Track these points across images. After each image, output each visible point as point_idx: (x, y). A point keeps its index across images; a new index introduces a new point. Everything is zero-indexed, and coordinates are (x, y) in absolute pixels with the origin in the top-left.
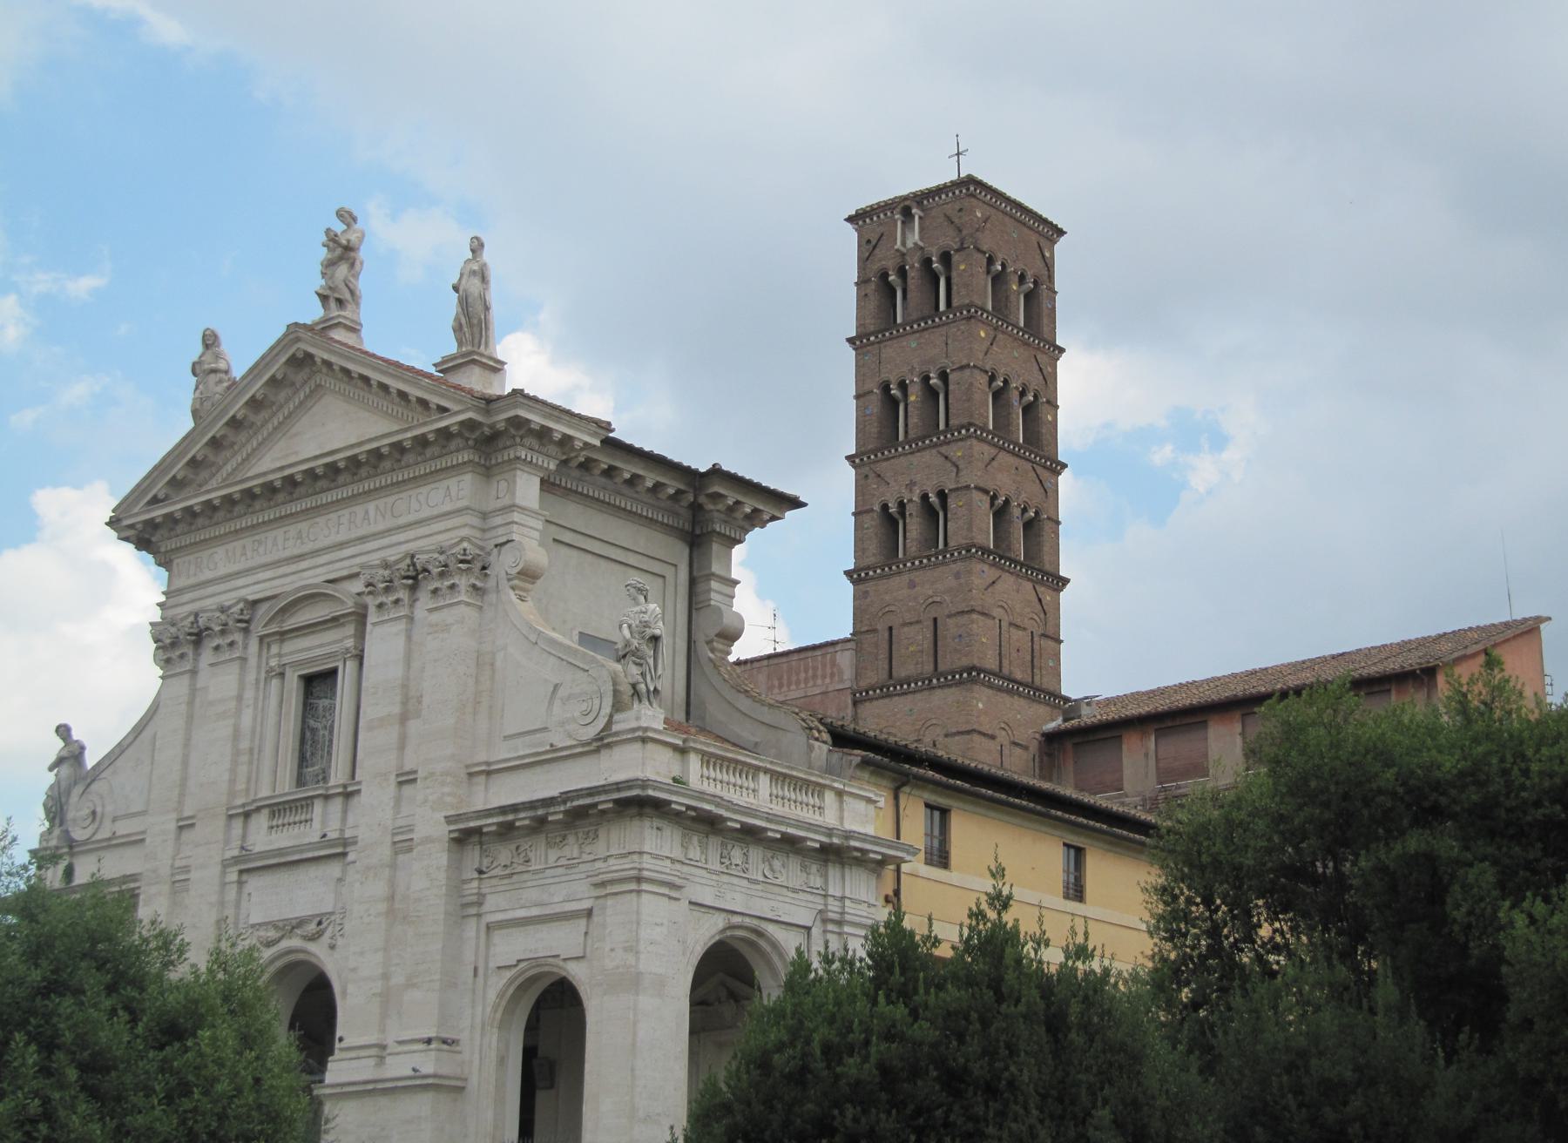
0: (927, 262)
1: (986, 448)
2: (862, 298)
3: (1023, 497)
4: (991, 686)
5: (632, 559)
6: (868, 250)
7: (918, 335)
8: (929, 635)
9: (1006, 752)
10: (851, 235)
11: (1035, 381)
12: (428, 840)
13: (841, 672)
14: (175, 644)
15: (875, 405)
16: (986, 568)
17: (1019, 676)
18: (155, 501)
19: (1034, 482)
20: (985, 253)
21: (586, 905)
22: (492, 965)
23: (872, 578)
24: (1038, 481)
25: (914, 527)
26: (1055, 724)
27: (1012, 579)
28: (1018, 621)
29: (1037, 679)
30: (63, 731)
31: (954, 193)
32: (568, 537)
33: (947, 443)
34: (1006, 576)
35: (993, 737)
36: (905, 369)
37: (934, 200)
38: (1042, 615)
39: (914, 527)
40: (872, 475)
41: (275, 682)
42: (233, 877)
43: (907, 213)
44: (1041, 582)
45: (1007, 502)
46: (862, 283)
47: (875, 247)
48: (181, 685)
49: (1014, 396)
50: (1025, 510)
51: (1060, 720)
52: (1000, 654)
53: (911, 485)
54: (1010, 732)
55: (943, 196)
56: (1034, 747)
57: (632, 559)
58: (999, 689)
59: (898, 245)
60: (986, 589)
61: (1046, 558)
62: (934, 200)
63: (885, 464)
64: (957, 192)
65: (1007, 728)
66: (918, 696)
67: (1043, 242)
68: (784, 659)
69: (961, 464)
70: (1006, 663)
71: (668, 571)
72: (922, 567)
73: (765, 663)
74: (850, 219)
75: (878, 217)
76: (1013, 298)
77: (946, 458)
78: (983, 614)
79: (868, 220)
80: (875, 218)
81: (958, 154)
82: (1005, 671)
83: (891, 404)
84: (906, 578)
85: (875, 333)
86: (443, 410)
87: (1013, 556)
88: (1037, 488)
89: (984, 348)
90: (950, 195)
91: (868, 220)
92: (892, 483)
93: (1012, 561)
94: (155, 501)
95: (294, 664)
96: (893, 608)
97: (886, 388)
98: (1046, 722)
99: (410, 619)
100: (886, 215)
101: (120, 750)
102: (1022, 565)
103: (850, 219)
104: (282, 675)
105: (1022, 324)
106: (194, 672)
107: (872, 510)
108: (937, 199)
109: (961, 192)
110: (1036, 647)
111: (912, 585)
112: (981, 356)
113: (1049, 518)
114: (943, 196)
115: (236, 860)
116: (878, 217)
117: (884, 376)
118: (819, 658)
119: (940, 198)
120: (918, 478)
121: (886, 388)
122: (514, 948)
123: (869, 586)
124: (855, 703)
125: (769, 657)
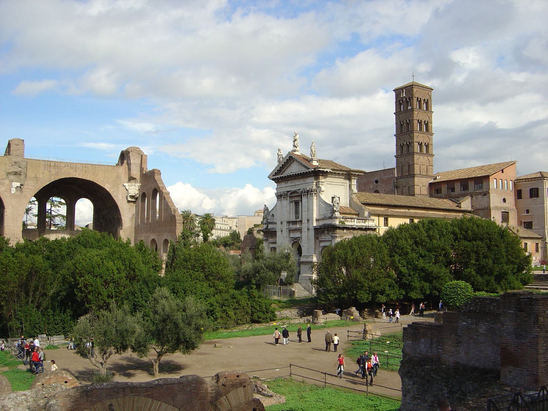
0: (406, 99)
1: (418, 134)
2: (396, 105)
3: (425, 141)
4: (418, 177)
5: (339, 184)
6: (397, 96)
9: (421, 188)
10: (394, 93)
11: (427, 119)
12: (311, 229)
14: (278, 196)
15: (399, 125)
16: (417, 156)
18: (273, 175)
21: (331, 239)
22: (320, 246)
25: (405, 148)
26: (432, 181)
27: (423, 157)
28: (424, 164)
29: (428, 174)
30: (265, 205)
32: (329, 183)
34: (421, 157)
36: (403, 119)
39: (405, 148)
41: (291, 203)
42: (288, 230)
43: (403, 90)
44: (429, 156)
45: (421, 143)
46: (396, 102)
48: (280, 202)
49: (423, 123)
50: (425, 144)
51: (433, 180)
56: (427, 186)
57: (339, 184)
58: (420, 177)
59: (402, 96)
61: (430, 151)
67: (429, 92)
71: (346, 184)
72: (406, 156)
74: (393, 90)
76: (422, 104)
77: (410, 136)
81: (413, 76)
82: (421, 173)
83: (402, 125)
84: (404, 157)
85: (398, 112)
86: (309, 168)
87: (423, 153)
93: (423, 154)
94: (273, 175)
95: (294, 201)
97: (400, 122)
98: (430, 181)
99: (308, 197)
101: (273, 209)
102: (426, 154)
103: (393, 90)
104: (292, 202)
105: (425, 109)
106: (281, 200)
111: (405, 159)
112: (416, 117)
115: (288, 228)
117: (400, 120)
120: (405, 139)
121: (400, 122)
122: (322, 244)
123: (398, 159)
124: (396, 179)
125: (383, 170)
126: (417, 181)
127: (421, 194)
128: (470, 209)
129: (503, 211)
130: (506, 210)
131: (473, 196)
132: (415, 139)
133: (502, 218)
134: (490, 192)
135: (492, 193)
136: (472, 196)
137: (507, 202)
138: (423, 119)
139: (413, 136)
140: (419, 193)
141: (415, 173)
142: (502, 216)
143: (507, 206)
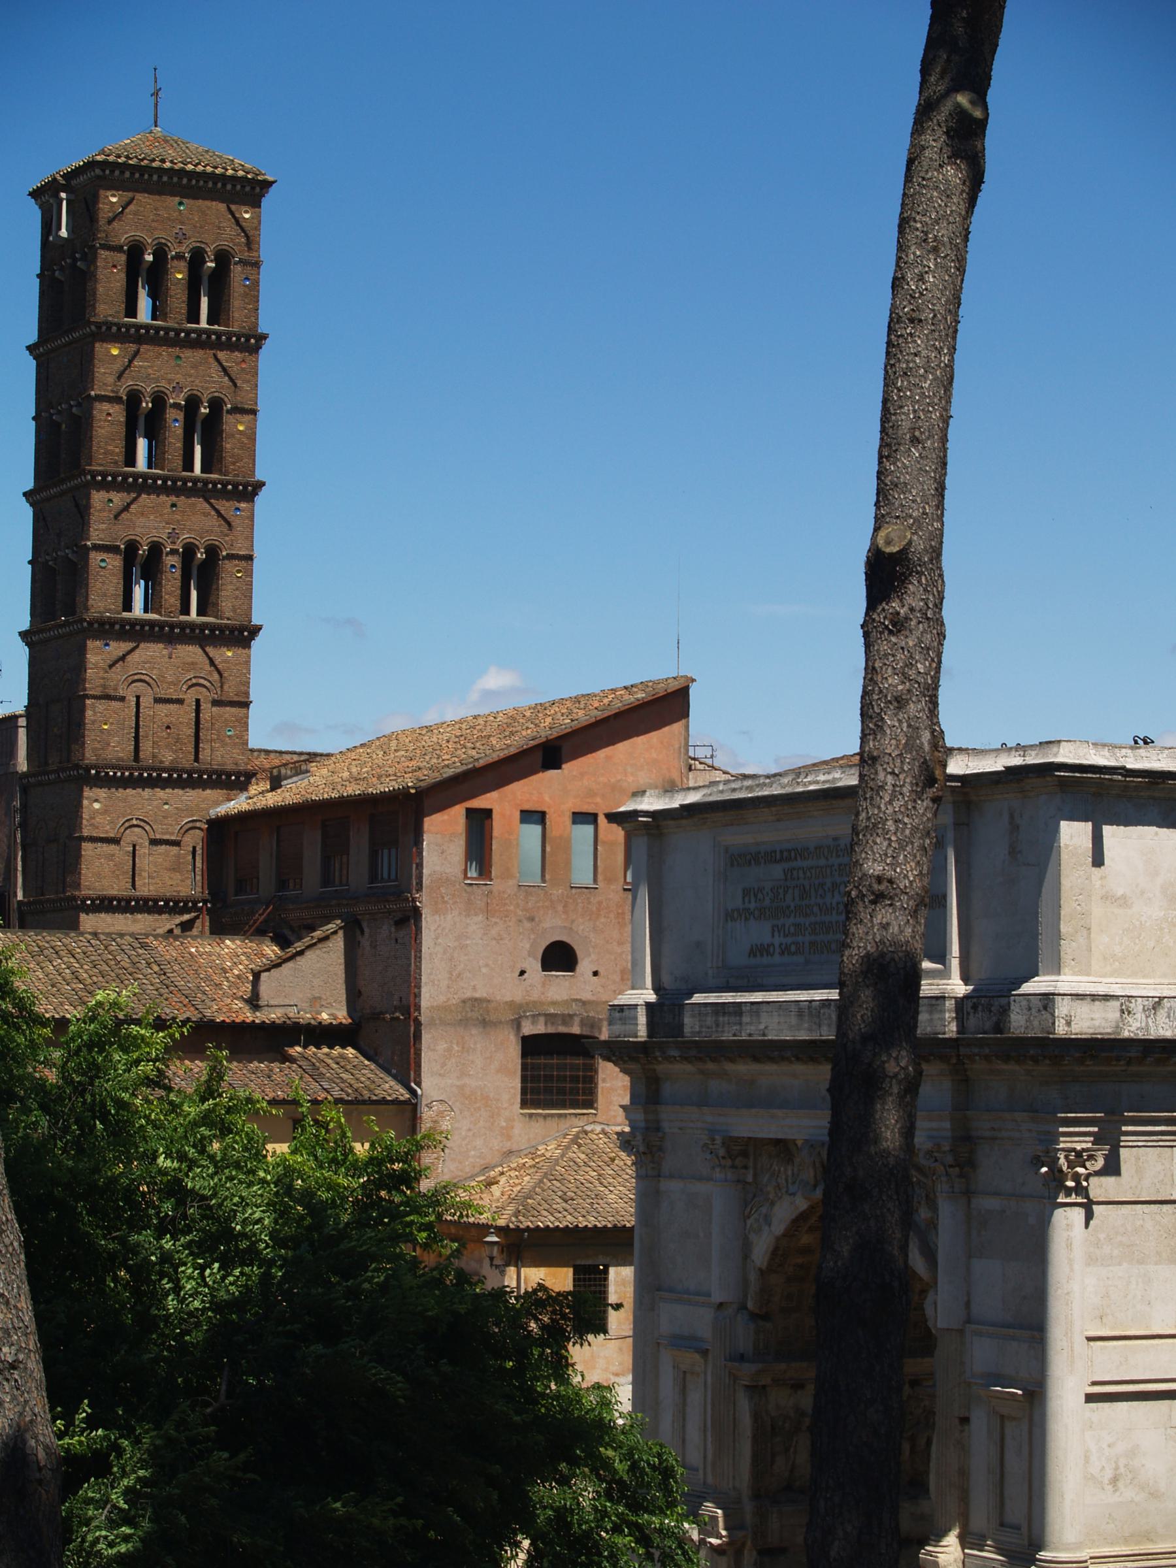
17: (168, 757)
19: (207, 515)
20: (119, 249)
24: (213, 513)
35: (115, 841)
38: (216, 676)
52: (137, 738)
54: (148, 828)
56: (195, 838)
60: (111, 666)
65: (142, 824)
70: (146, 748)
78: (108, 697)
88: (213, 521)
89: (118, 366)
110: (205, 716)
112: (111, 380)
113: (231, 557)
126: (105, 811)
127: (145, 888)
128: (334, 1012)
129: (540, 1028)
130: (567, 1019)
131: (365, 925)
132: (98, 532)
133: (524, 1079)
134: (425, 901)
135: (436, 912)
136: (353, 931)
137: (585, 966)
138: (178, 388)
139: (88, 506)
140: (117, 887)
141: (90, 757)
142: (524, 1067)
143: (586, 996)
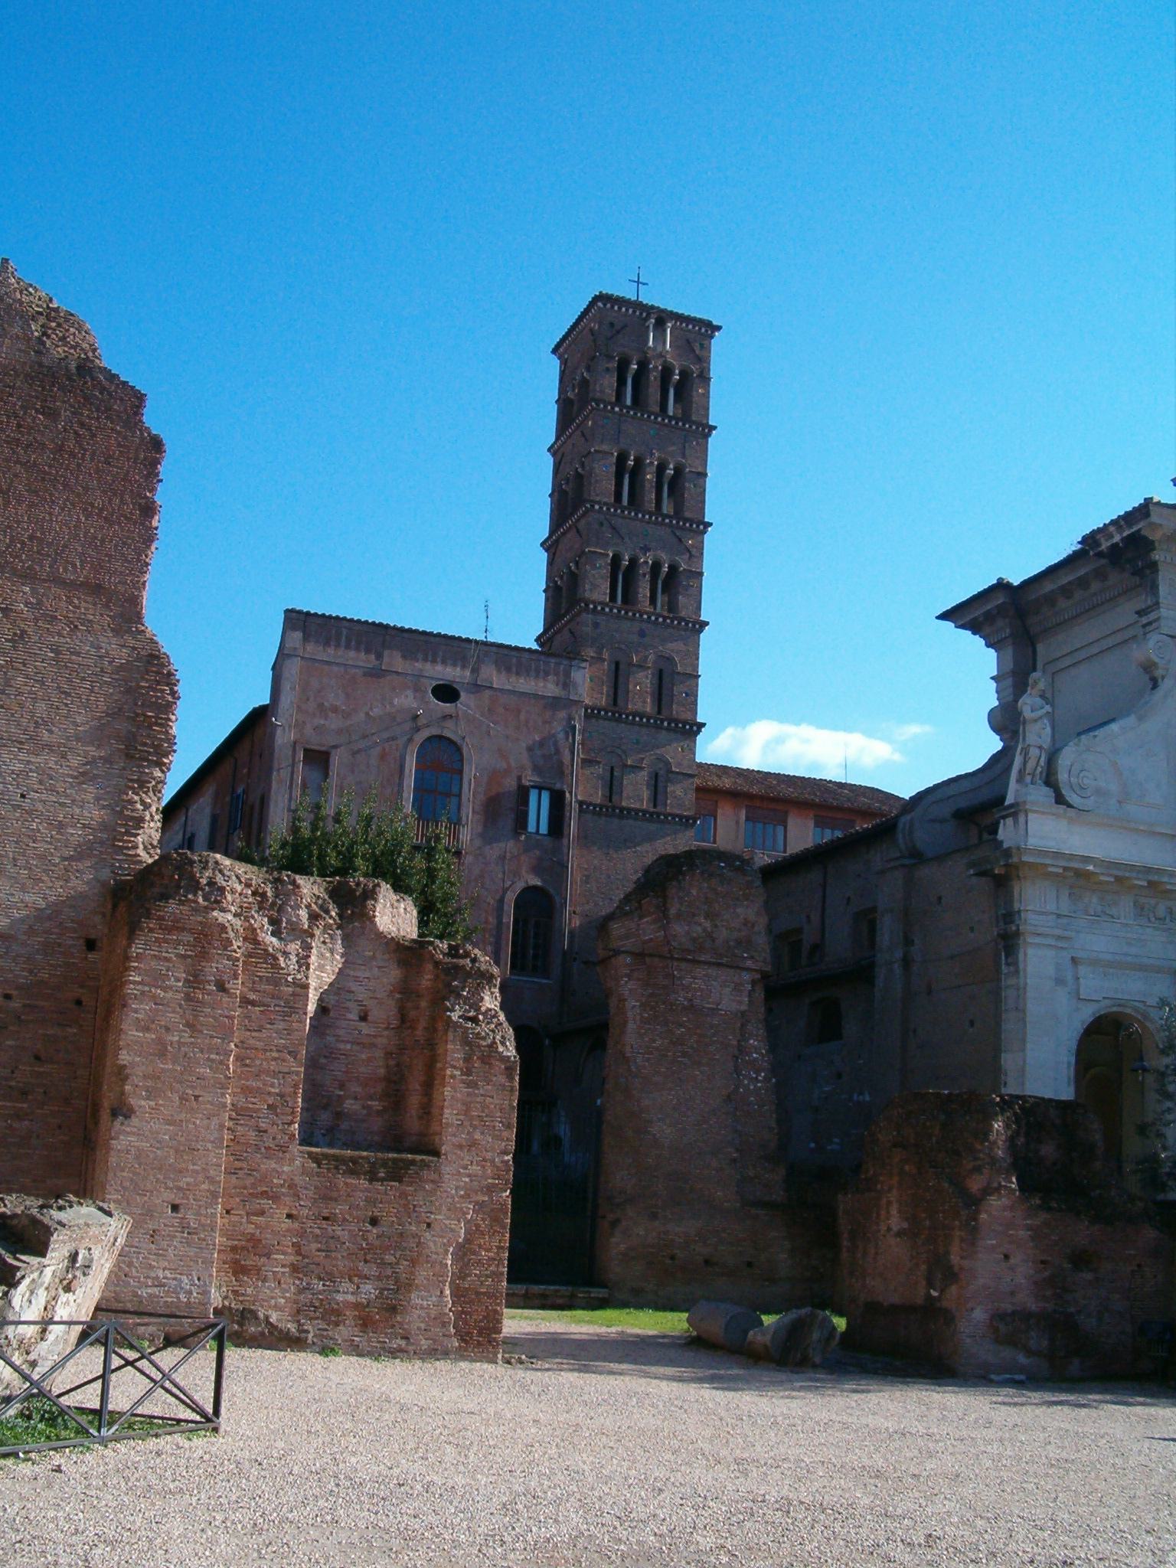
7: (657, 426)
8: (656, 681)
13: (575, 686)
23: (606, 614)
31: (700, 329)
33: (683, 529)
37: (681, 324)
40: (605, 522)
43: (660, 323)
47: (618, 332)
53: (646, 549)
55: (690, 327)
62: (681, 324)
63: (620, 520)
64: (703, 330)
66: (644, 730)
68: (513, 653)
69: (694, 551)
73: (494, 649)
75: (627, 310)
79: (616, 308)
80: (624, 309)
90: (697, 328)
91: (616, 308)
92: (627, 540)
96: (623, 647)
100: (634, 312)
107: (608, 555)
108: (684, 325)
109: (706, 331)
114: (690, 327)
116: (627, 310)
118: (552, 665)
119: (687, 325)
